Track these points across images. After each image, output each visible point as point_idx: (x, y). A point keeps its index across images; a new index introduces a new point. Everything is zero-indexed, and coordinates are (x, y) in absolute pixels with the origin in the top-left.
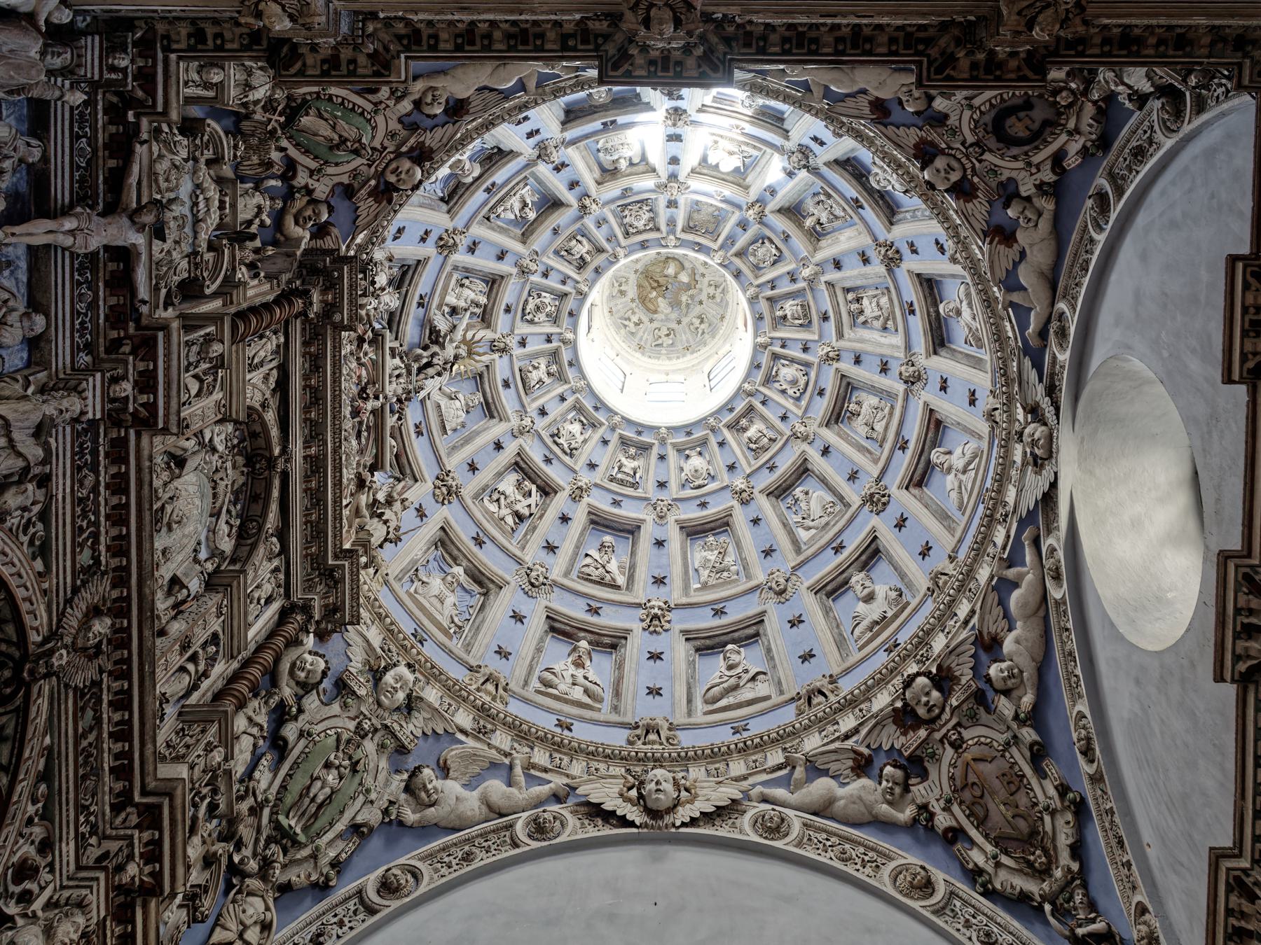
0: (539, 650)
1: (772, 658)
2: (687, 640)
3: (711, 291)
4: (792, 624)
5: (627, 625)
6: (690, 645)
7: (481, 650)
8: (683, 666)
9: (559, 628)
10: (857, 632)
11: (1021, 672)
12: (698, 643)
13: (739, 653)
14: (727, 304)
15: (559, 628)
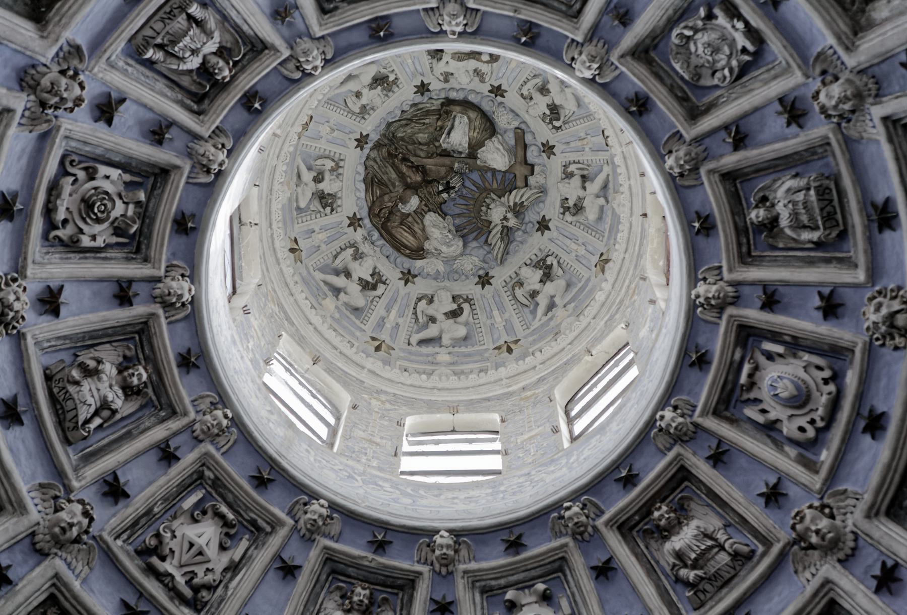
3: (572, 191)
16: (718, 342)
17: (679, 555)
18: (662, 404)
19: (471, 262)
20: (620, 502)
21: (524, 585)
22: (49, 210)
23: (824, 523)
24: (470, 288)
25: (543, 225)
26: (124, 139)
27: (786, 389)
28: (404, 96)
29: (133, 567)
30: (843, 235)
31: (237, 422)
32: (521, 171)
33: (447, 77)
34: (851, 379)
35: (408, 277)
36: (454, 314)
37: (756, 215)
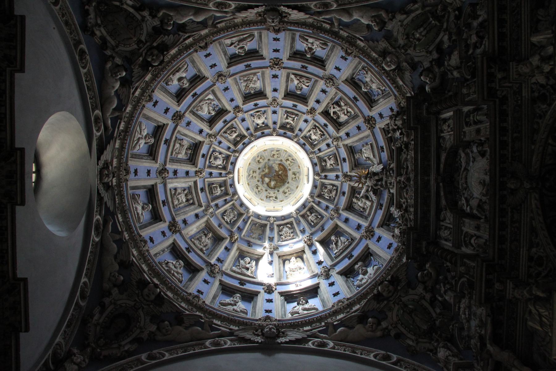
0: (328, 56)
1: (223, 52)
2: (262, 56)
3: (255, 175)
4: (215, 65)
5: (289, 62)
6: (261, 54)
7: (353, 61)
8: (263, 47)
9: (320, 62)
10: (186, 66)
11: (112, 75)
12: (257, 55)
13: (239, 52)
14: (247, 172)
15: (320, 62)
16: (230, 166)
17: (235, 132)
18: (238, 156)
19: (271, 162)
20: (246, 140)
21: (262, 127)
22: (337, 192)
23: (212, 139)
24: (271, 159)
25: (259, 169)
26: (324, 203)
27: (218, 160)
28: (281, 190)
29: (325, 133)
30: (209, 185)
31: (308, 155)
32: (263, 177)
33: (274, 193)
34: (207, 163)
35: (281, 160)
36: (274, 155)
37: (223, 188)
